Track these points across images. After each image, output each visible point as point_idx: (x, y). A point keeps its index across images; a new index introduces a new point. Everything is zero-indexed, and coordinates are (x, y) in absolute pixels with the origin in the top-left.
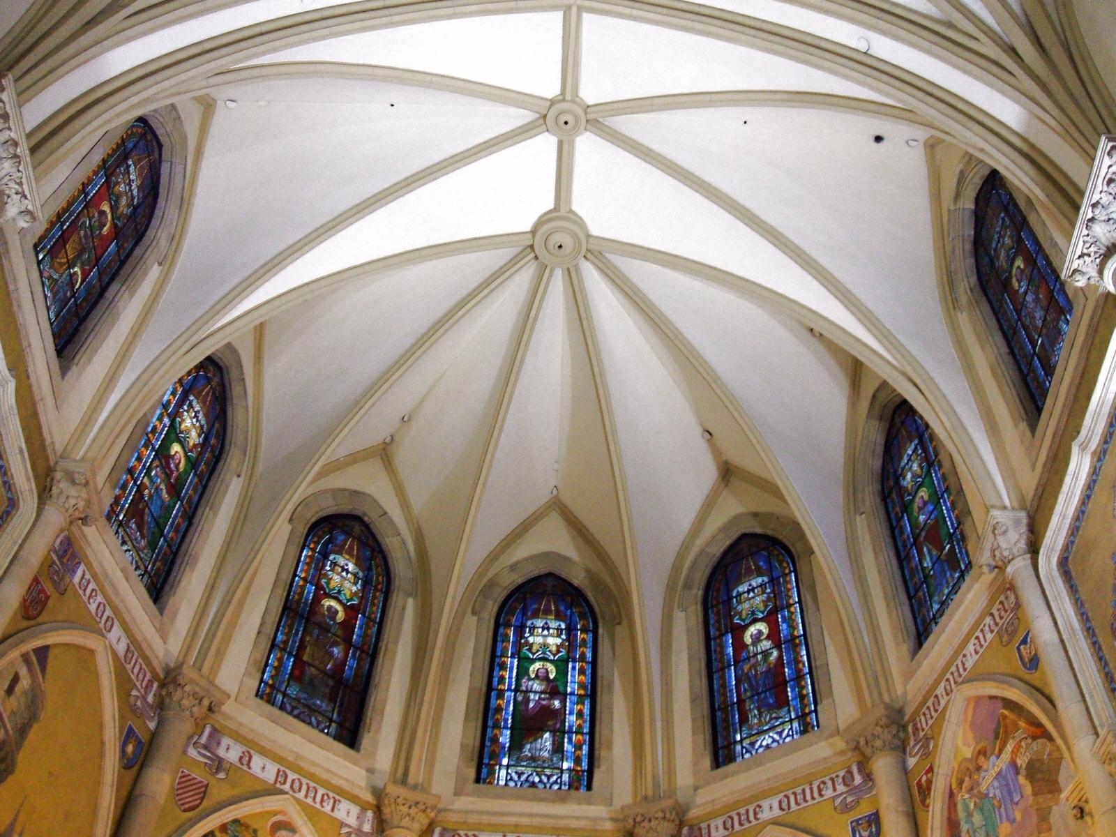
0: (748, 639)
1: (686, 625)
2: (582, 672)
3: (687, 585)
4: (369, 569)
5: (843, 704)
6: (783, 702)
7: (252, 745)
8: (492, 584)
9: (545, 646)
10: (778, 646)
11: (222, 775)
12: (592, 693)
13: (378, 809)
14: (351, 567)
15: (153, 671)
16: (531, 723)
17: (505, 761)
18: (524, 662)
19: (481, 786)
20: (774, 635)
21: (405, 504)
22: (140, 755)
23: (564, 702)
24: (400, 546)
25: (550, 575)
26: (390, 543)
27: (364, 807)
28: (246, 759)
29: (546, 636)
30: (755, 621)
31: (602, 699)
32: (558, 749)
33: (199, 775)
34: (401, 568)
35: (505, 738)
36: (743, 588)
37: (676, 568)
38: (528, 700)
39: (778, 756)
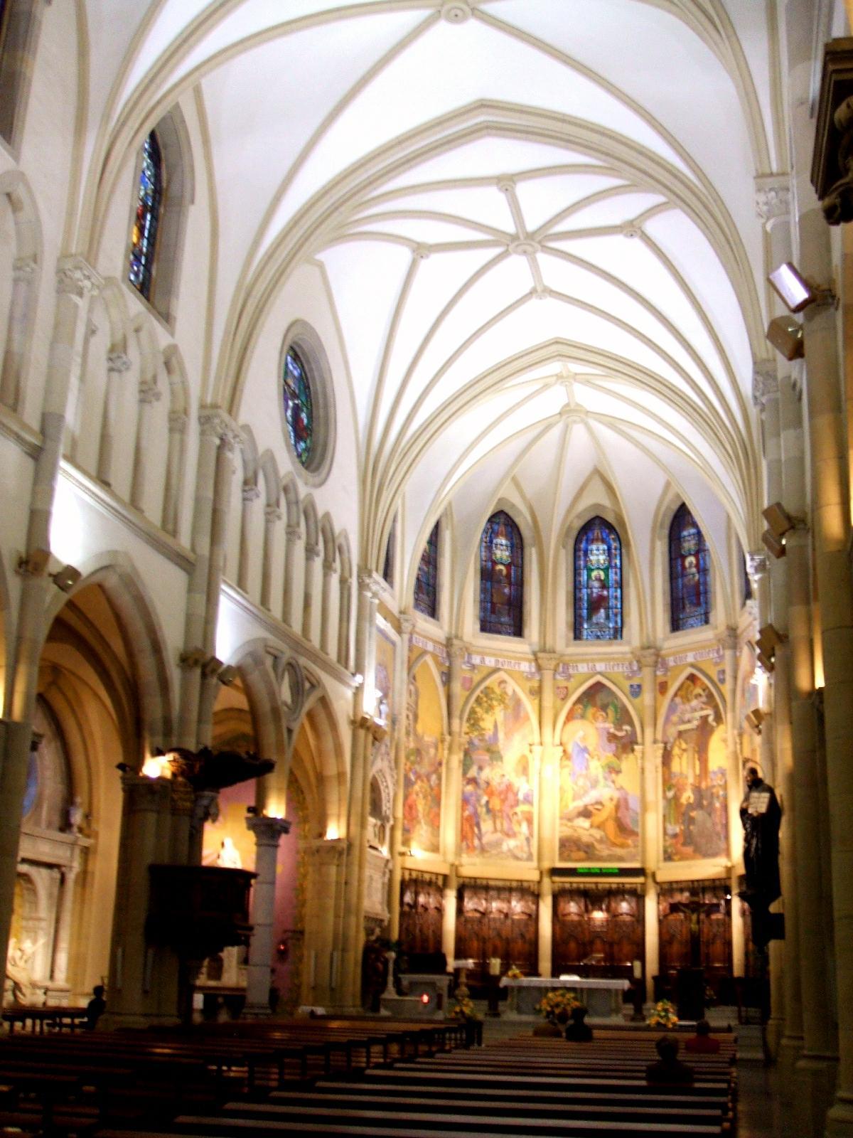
0: (687, 564)
1: (661, 547)
2: (616, 574)
3: (662, 526)
4: (512, 538)
5: (719, 615)
6: (698, 604)
7: (483, 654)
8: (570, 528)
9: (598, 561)
10: (699, 572)
11: (476, 671)
12: (620, 585)
13: (536, 660)
14: (504, 542)
15: (441, 644)
16: (597, 604)
17: (585, 626)
18: (590, 570)
19: (578, 642)
20: (697, 566)
21: (523, 496)
22: (448, 677)
23: (608, 592)
24: (523, 521)
25: (597, 517)
26: (518, 520)
27: (530, 661)
28: (483, 660)
29: (598, 555)
30: (690, 554)
31: (624, 590)
32: (607, 617)
33: (468, 675)
34: (526, 532)
35: (585, 612)
36: (685, 533)
37: (658, 508)
38: (592, 592)
39: (696, 636)
